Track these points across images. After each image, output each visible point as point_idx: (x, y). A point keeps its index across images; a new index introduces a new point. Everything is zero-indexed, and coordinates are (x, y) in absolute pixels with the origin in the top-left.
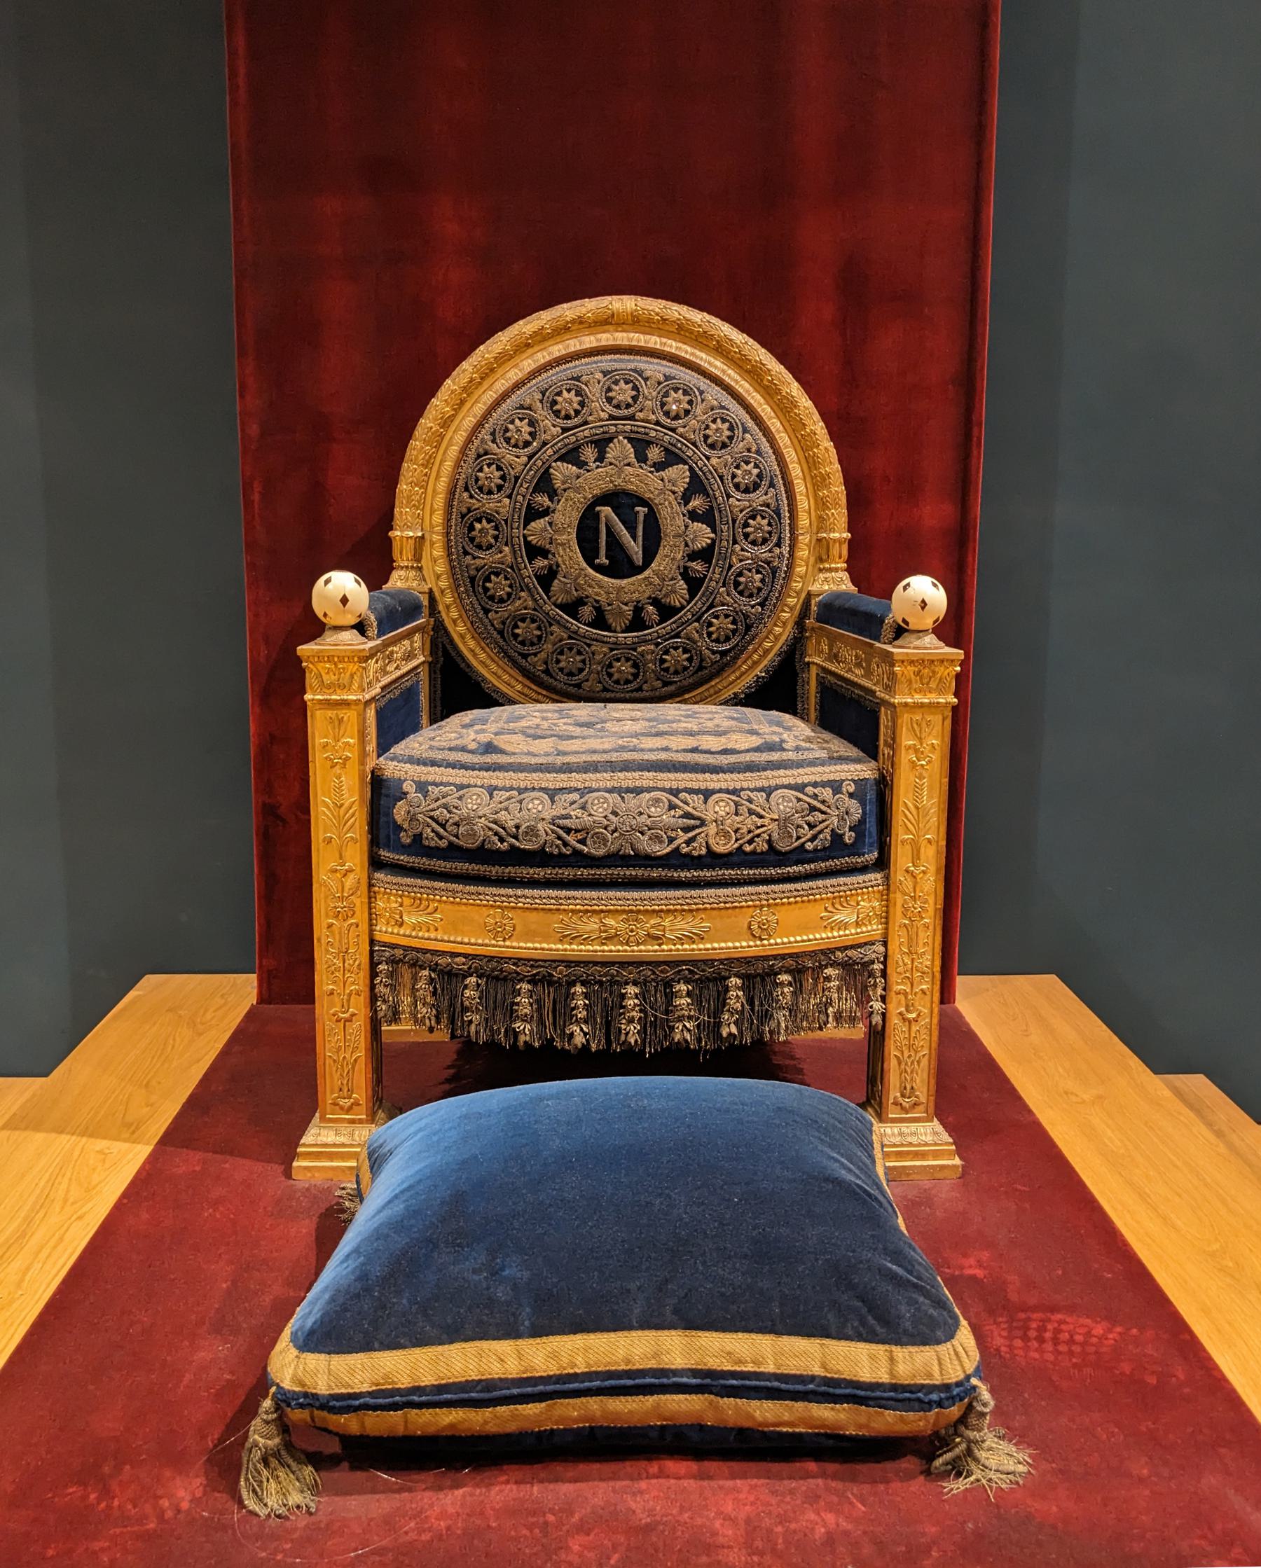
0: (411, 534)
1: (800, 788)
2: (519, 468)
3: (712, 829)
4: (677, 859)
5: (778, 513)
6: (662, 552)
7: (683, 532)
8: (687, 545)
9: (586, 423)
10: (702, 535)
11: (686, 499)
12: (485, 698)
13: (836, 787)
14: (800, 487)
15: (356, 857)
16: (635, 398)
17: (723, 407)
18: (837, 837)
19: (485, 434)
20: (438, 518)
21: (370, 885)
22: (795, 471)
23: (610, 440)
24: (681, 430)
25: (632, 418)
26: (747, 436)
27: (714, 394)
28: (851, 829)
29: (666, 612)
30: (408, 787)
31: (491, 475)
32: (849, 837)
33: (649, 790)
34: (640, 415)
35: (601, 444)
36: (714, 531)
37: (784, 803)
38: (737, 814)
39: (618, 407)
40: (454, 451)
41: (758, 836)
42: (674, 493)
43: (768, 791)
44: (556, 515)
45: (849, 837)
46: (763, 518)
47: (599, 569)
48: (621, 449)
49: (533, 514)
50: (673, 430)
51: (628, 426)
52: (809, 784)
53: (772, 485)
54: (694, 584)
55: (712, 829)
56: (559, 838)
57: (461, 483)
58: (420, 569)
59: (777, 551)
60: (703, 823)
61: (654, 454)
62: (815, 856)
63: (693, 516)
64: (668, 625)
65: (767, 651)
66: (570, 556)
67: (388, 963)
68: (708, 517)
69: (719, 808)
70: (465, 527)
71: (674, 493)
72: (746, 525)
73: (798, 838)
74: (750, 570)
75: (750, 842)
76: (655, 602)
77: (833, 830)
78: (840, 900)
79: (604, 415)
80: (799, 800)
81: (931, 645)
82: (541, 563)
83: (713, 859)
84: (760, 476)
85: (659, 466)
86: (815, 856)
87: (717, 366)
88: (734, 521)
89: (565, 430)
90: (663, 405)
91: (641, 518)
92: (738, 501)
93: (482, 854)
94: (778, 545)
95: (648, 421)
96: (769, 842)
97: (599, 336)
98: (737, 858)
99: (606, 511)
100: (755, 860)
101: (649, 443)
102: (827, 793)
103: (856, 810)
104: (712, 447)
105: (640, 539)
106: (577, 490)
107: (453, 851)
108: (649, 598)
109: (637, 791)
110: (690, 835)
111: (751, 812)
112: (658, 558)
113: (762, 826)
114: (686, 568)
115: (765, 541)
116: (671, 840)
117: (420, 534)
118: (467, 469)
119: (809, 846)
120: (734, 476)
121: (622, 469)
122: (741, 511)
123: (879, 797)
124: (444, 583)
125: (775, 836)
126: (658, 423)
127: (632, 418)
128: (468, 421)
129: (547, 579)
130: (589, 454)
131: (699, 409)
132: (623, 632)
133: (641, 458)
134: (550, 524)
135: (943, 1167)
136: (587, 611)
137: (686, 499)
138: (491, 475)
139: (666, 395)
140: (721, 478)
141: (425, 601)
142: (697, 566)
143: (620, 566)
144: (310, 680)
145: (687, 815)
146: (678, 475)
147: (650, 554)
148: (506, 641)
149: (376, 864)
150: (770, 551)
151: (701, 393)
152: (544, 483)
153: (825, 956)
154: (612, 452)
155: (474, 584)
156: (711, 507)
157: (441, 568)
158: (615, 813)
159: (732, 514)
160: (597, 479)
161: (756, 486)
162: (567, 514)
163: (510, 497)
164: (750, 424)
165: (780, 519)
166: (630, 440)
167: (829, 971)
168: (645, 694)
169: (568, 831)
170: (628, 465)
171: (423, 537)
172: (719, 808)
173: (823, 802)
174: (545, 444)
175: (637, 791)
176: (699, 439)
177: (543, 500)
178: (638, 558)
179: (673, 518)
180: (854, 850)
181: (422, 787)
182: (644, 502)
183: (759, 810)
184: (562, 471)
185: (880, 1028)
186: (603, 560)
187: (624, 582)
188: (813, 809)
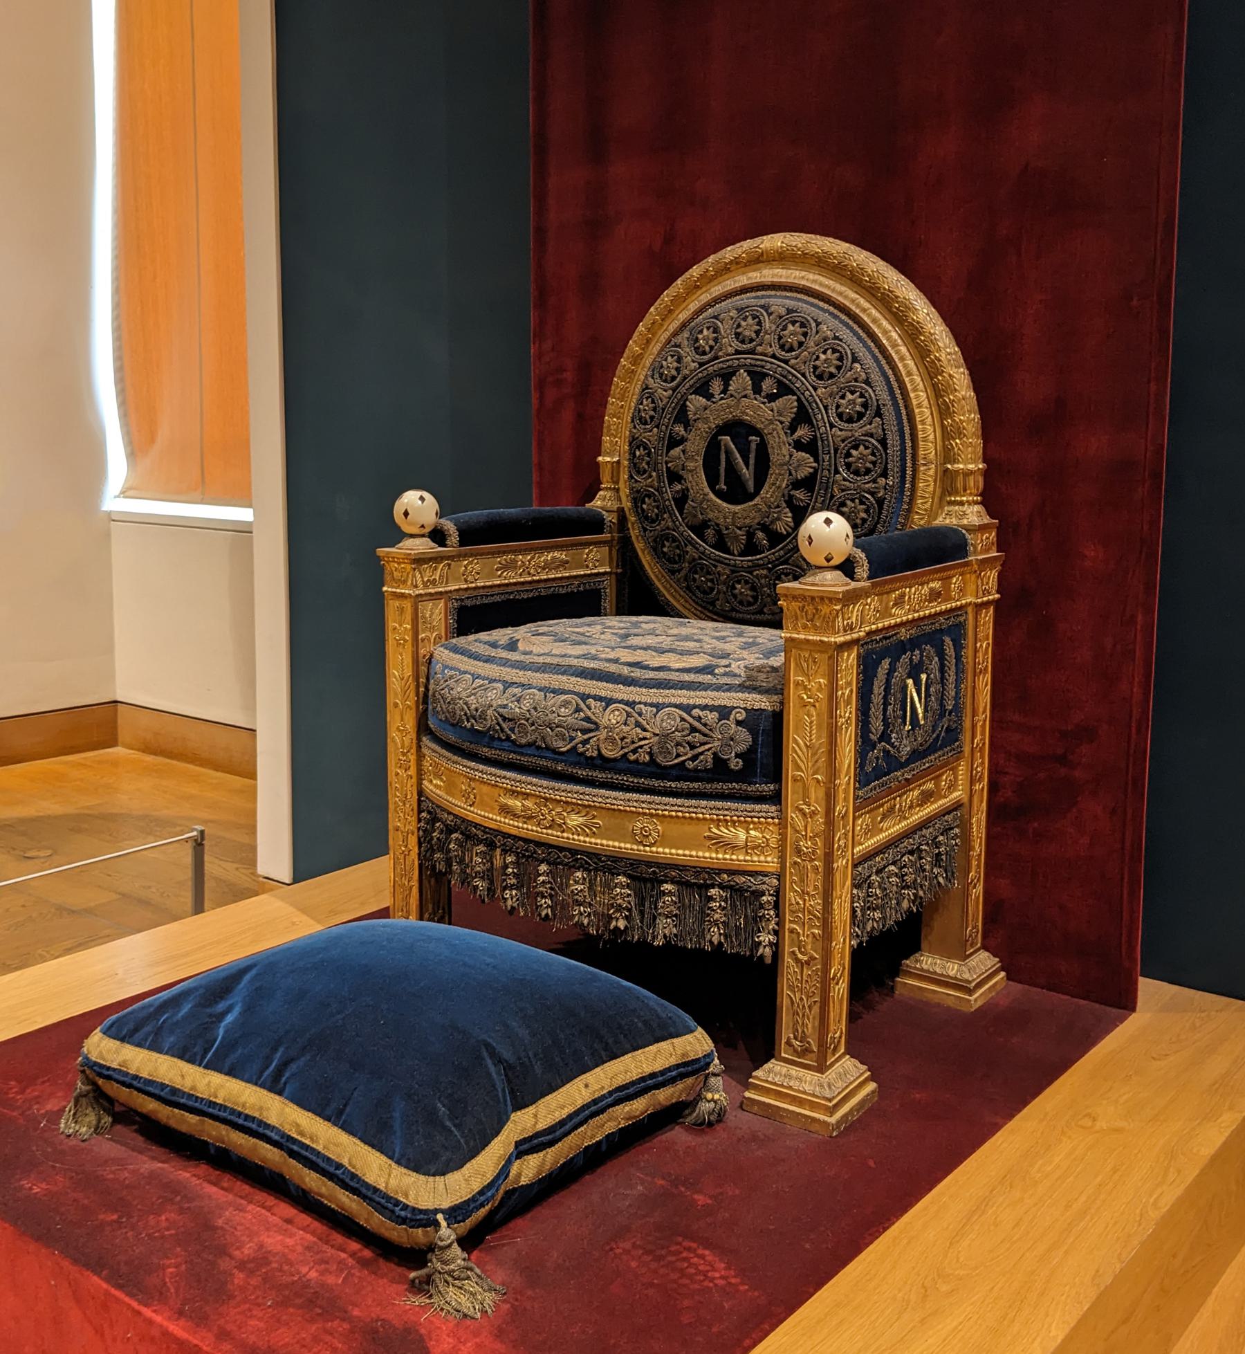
0: (608, 459)
1: (688, 709)
2: (665, 401)
3: (603, 736)
5: (883, 442)
6: (771, 479)
8: (790, 474)
9: (716, 358)
10: (805, 463)
13: (724, 712)
15: (410, 724)
16: (757, 333)
17: (836, 338)
21: (419, 747)
23: (733, 373)
24: (793, 361)
25: (752, 352)
26: (857, 365)
28: (737, 756)
32: (736, 764)
33: (564, 692)
34: (759, 349)
36: (816, 460)
37: (668, 721)
38: (625, 724)
39: (743, 342)
41: (641, 747)
42: (782, 423)
43: (658, 707)
44: (688, 444)
45: (736, 764)
46: (866, 448)
47: (719, 494)
48: (742, 380)
49: (674, 442)
50: (786, 362)
51: (748, 359)
52: (695, 707)
53: (878, 414)
55: (603, 734)
56: (498, 724)
58: (618, 490)
59: (882, 481)
60: (597, 729)
61: (768, 385)
62: (695, 776)
63: (799, 445)
64: (778, 551)
66: (698, 482)
68: (810, 447)
69: (612, 717)
71: (782, 423)
72: (848, 455)
73: (678, 756)
74: (853, 501)
75: (634, 751)
76: (764, 528)
77: (715, 754)
79: (730, 350)
80: (683, 719)
83: (602, 762)
85: (772, 398)
86: (695, 776)
88: (836, 450)
89: (701, 364)
90: (780, 338)
91: (753, 446)
94: (884, 474)
95: (765, 355)
96: (650, 754)
97: (750, 275)
100: (636, 769)
101: (765, 375)
102: (711, 717)
103: (744, 739)
104: (820, 377)
105: (751, 467)
106: (706, 420)
108: (759, 524)
109: (556, 692)
110: (586, 737)
111: (638, 724)
112: (766, 486)
113: (645, 739)
114: (791, 497)
115: (868, 471)
116: (572, 739)
117: (616, 459)
119: (690, 765)
120: (838, 407)
122: (843, 441)
125: (655, 748)
126: (774, 356)
127: (752, 352)
132: (740, 555)
133: (757, 389)
134: (684, 451)
135: (814, 1120)
137: (793, 428)
139: (785, 328)
140: (826, 408)
143: (736, 493)
145: (587, 719)
146: (789, 402)
150: (874, 481)
151: (818, 324)
152: (682, 416)
156: (815, 436)
158: (535, 708)
161: (861, 416)
162: (696, 444)
163: (657, 427)
166: (749, 373)
167: (668, 887)
168: (767, 617)
169: (504, 719)
170: (745, 396)
171: (618, 462)
172: (612, 717)
173: (705, 725)
174: (685, 378)
175: (556, 692)
176: (808, 370)
177: (680, 429)
178: (751, 485)
179: (781, 448)
180: (743, 776)
182: (757, 432)
183: (644, 723)
185: (768, 960)
187: (737, 508)
188: (694, 730)
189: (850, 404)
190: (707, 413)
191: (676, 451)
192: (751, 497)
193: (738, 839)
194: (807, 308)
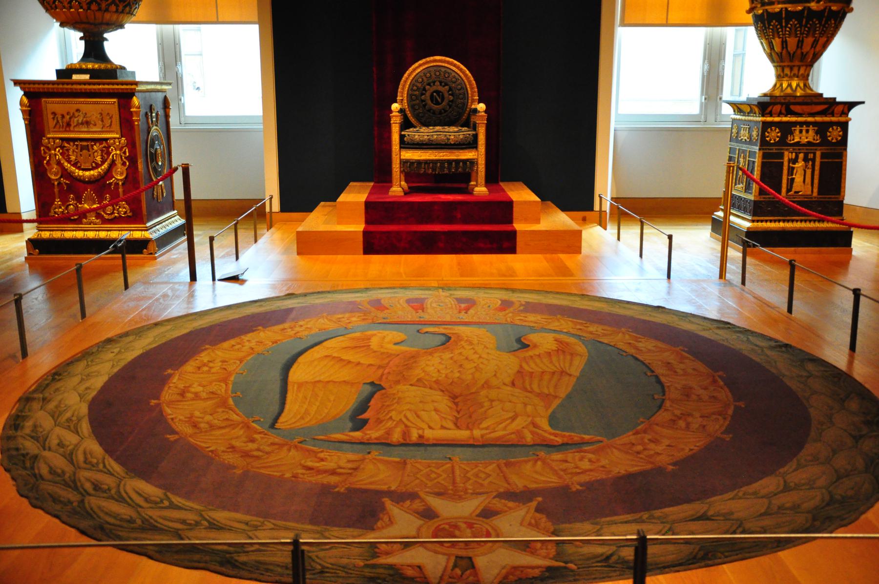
4: (446, 144)
10: (451, 98)
12: (415, 127)
15: (398, 147)
27: (453, 74)
29: (445, 111)
35: (434, 83)
37: (461, 137)
48: (437, 83)
49: (422, 94)
66: (429, 102)
67: (404, 163)
70: (410, 97)
83: (451, 144)
87: (454, 68)
93: (418, 144)
98: (454, 144)
107: (414, 144)
123: (476, 137)
129: (425, 106)
138: (415, 88)
143: (437, 103)
146: (447, 87)
149: (401, 148)
152: (424, 89)
153: (467, 160)
155: (412, 107)
159: (459, 94)
160: (434, 88)
162: (428, 94)
165: (465, 96)
179: (446, 95)
184: (428, 87)
190: (430, 89)
193: (468, 155)
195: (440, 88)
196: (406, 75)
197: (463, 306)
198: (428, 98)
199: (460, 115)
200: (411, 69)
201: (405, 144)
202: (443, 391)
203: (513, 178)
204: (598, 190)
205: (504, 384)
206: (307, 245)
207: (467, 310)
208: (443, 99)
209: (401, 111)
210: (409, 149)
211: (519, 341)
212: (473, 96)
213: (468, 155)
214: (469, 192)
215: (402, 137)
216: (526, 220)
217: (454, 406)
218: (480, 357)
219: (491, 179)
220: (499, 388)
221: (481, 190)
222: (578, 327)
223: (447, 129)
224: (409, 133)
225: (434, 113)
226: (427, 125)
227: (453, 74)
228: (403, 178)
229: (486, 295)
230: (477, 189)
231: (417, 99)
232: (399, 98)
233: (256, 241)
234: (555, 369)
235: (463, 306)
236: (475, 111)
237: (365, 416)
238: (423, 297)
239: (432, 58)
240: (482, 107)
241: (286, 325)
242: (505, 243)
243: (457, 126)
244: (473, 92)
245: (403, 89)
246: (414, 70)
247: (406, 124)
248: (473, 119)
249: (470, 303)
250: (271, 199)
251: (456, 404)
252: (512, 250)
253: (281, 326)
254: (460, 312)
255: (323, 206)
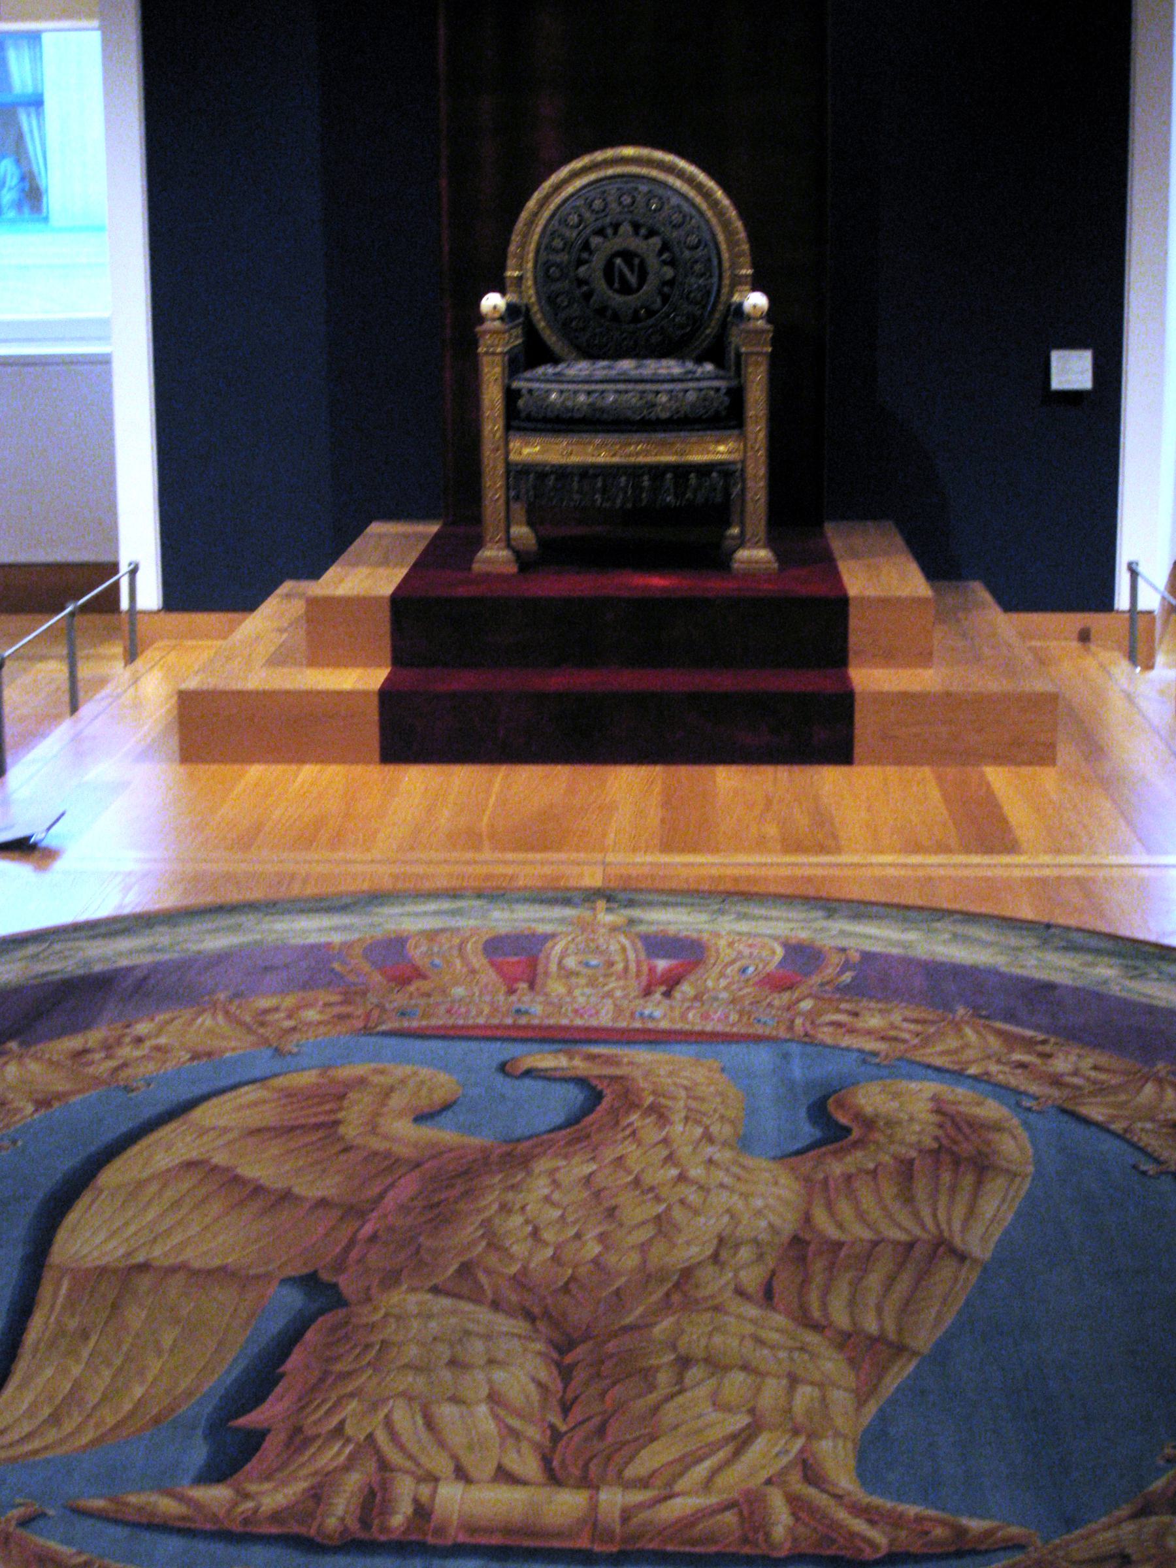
1: (701, 390)
6: (648, 282)
7: (659, 271)
10: (669, 272)
11: (660, 253)
12: (556, 361)
13: (718, 390)
14: (723, 247)
18: (717, 412)
19: (555, 222)
20: (530, 265)
22: (721, 238)
29: (651, 313)
30: (524, 392)
31: (558, 243)
35: (616, 227)
37: (691, 396)
40: (539, 229)
48: (626, 228)
49: (580, 262)
53: (706, 245)
54: (665, 299)
57: (543, 247)
61: (643, 231)
63: (664, 263)
64: (651, 322)
65: (708, 335)
66: (601, 285)
68: (672, 263)
69: (664, 398)
70: (545, 273)
78: (718, 442)
81: (760, 323)
82: (585, 288)
84: (700, 241)
85: (647, 237)
87: (678, 184)
92: (687, 254)
99: (618, 261)
102: (712, 393)
107: (545, 420)
109: (626, 392)
118: (545, 241)
121: (625, 239)
123: (737, 396)
124: (533, 299)
128: (546, 214)
129: (588, 296)
130: (609, 231)
131: (666, 207)
136: (609, 313)
138: (558, 243)
141: (524, 309)
142: (666, 289)
143: (626, 289)
144: (481, 342)
146: (656, 241)
147: (640, 286)
148: (565, 329)
149: (508, 428)
152: (586, 246)
154: (622, 230)
155: (550, 300)
157: (532, 292)
160: (617, 244)
164: (694, 213)
165: (711, 266)
179: (653, 263)
181: (530, 391)
184: (595, 241)
186: (616, 285)
189: (693, 239)
190: (603, 247)
191: (582, 269)
192: (638, 290)
193: (721, 450)
194: (661, 191)
195: (635, 244)
196: (531, 204)
197: (662, 964)
198: (599, 274)
199: (697, 323)
200: (547, 185)
201: (522, 418)
202: (530, 1317)
203: (865, 507)
204: (1128, 548)
205: (740, 1292)
206: (209, 730)
207: (671, 983)
208: (643, 276)
209: (512, 311)
210: (552, 422)
211: (819, 1111)
212: (734, 265)
213: (721, 450)
214: (716, 558)
215: (511, 396)
216: (889, 657)
217: (556, 1385)
218: (682, 1178)
219: (799, 513)
220: (717, 1309)
221: (755, 555)
222: (1017, 1056)
223: (652, 367)
224: (529, 382)
225: (616, 317)
226: (590, 353)
227: (674, 200)
228: (518, 510)
229: (744, 926)
230: (743, 554)
231: (563, 276)
232: (512, 273)
233: (74, 708)
234: (918, 1232)
235: (662, 964)
236: (738, 311)
237: (253, 1419)
238: (541, 928)
239: (609, 153)
240: (757, 301)
241: (94, 1037)
242: (820, 730)
243: (681, 357)
244: (735, 257)
245: (523, 245)
246: (557, 188)
247: (532, 353)
248: (735, 338)
249: (689, 954)
250: (133, 572)
251: (566, 1373)
252: (841, 752)
253: (74, 1043)
254: (647, 992)
255: (288, 596)
